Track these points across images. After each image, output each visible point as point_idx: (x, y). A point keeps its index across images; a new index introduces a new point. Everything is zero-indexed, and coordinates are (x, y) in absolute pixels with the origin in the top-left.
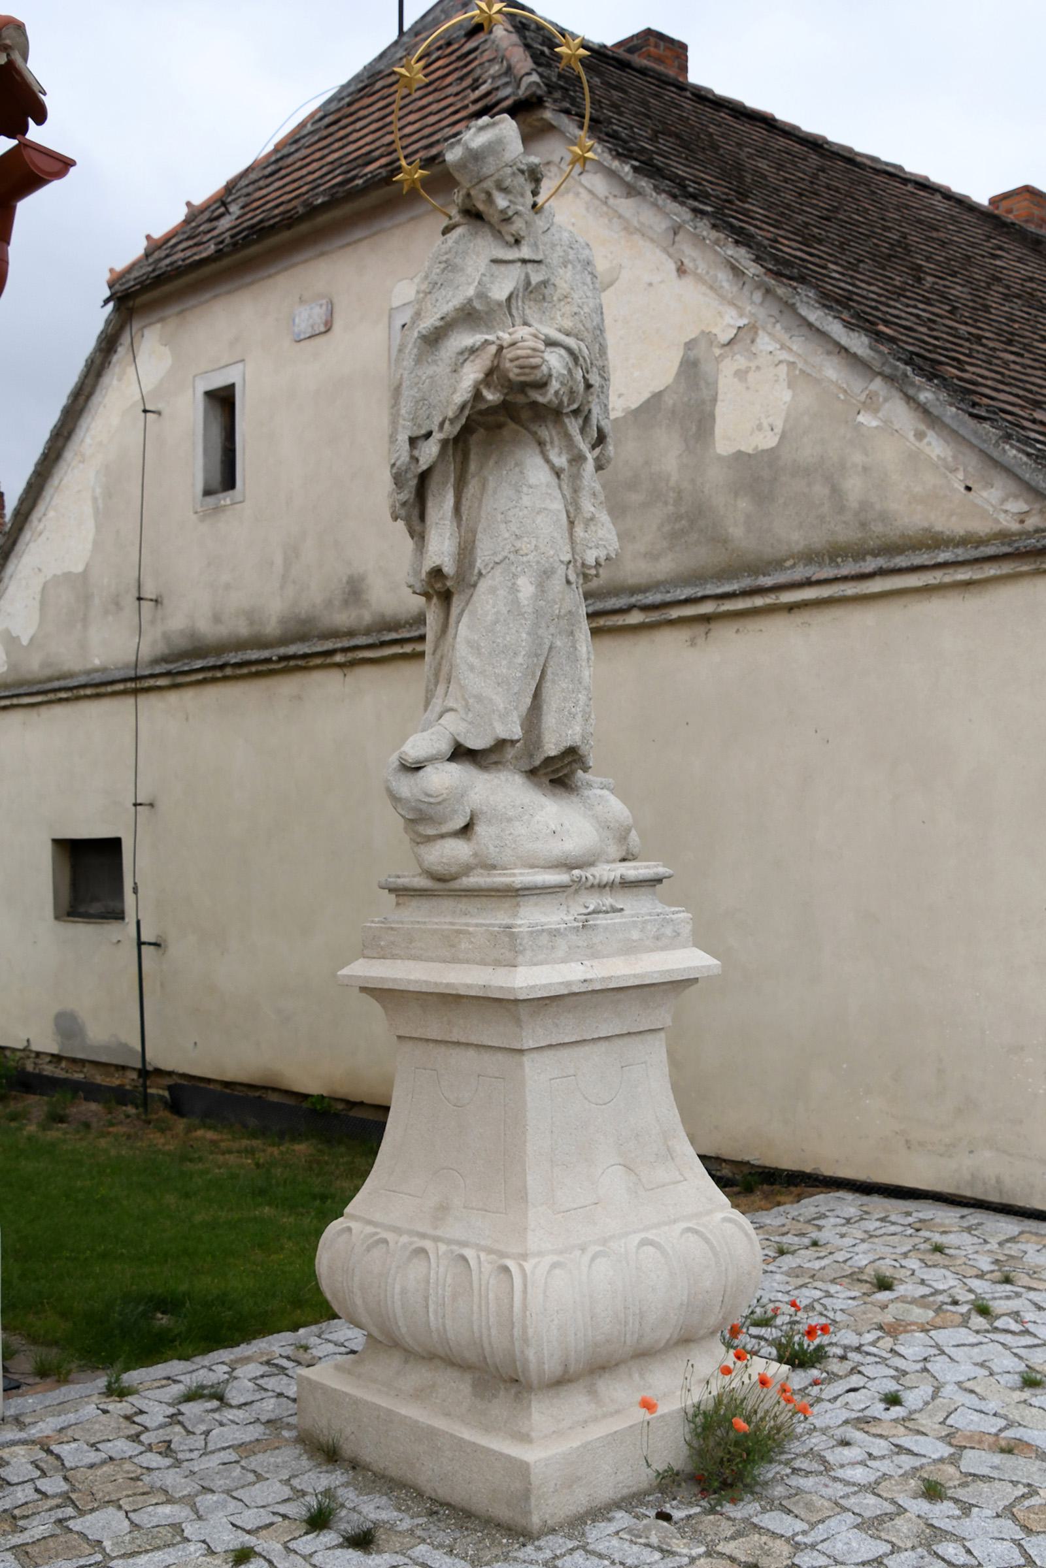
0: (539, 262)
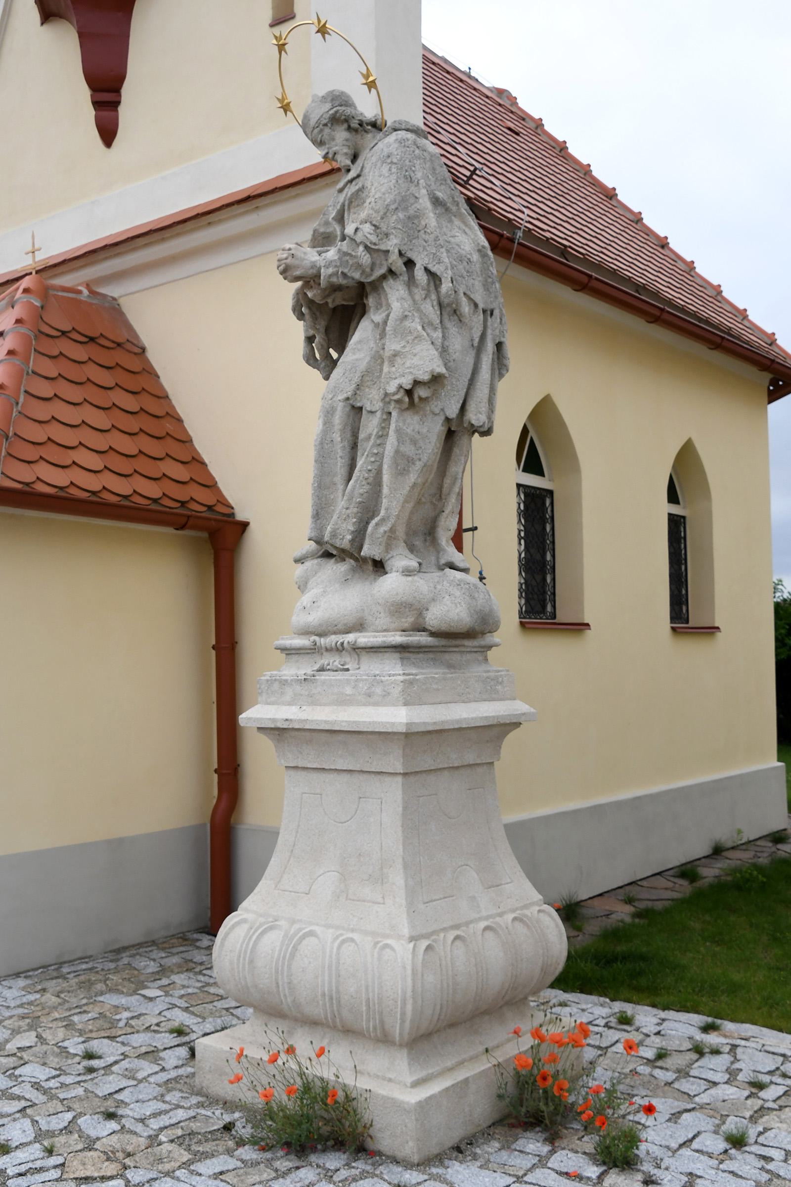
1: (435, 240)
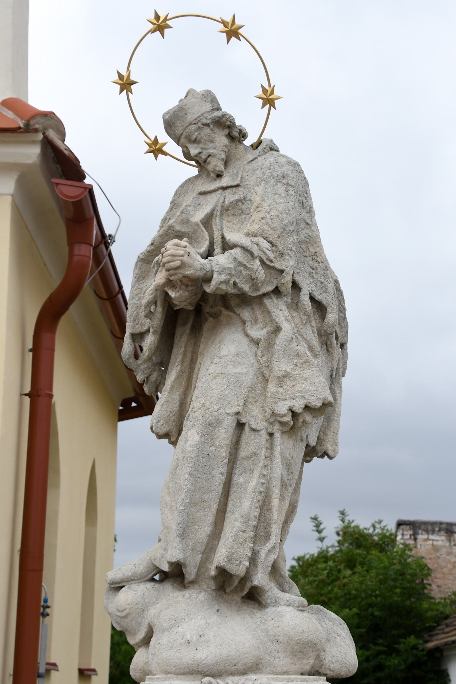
0: (238, 186)
1: (324, 269)
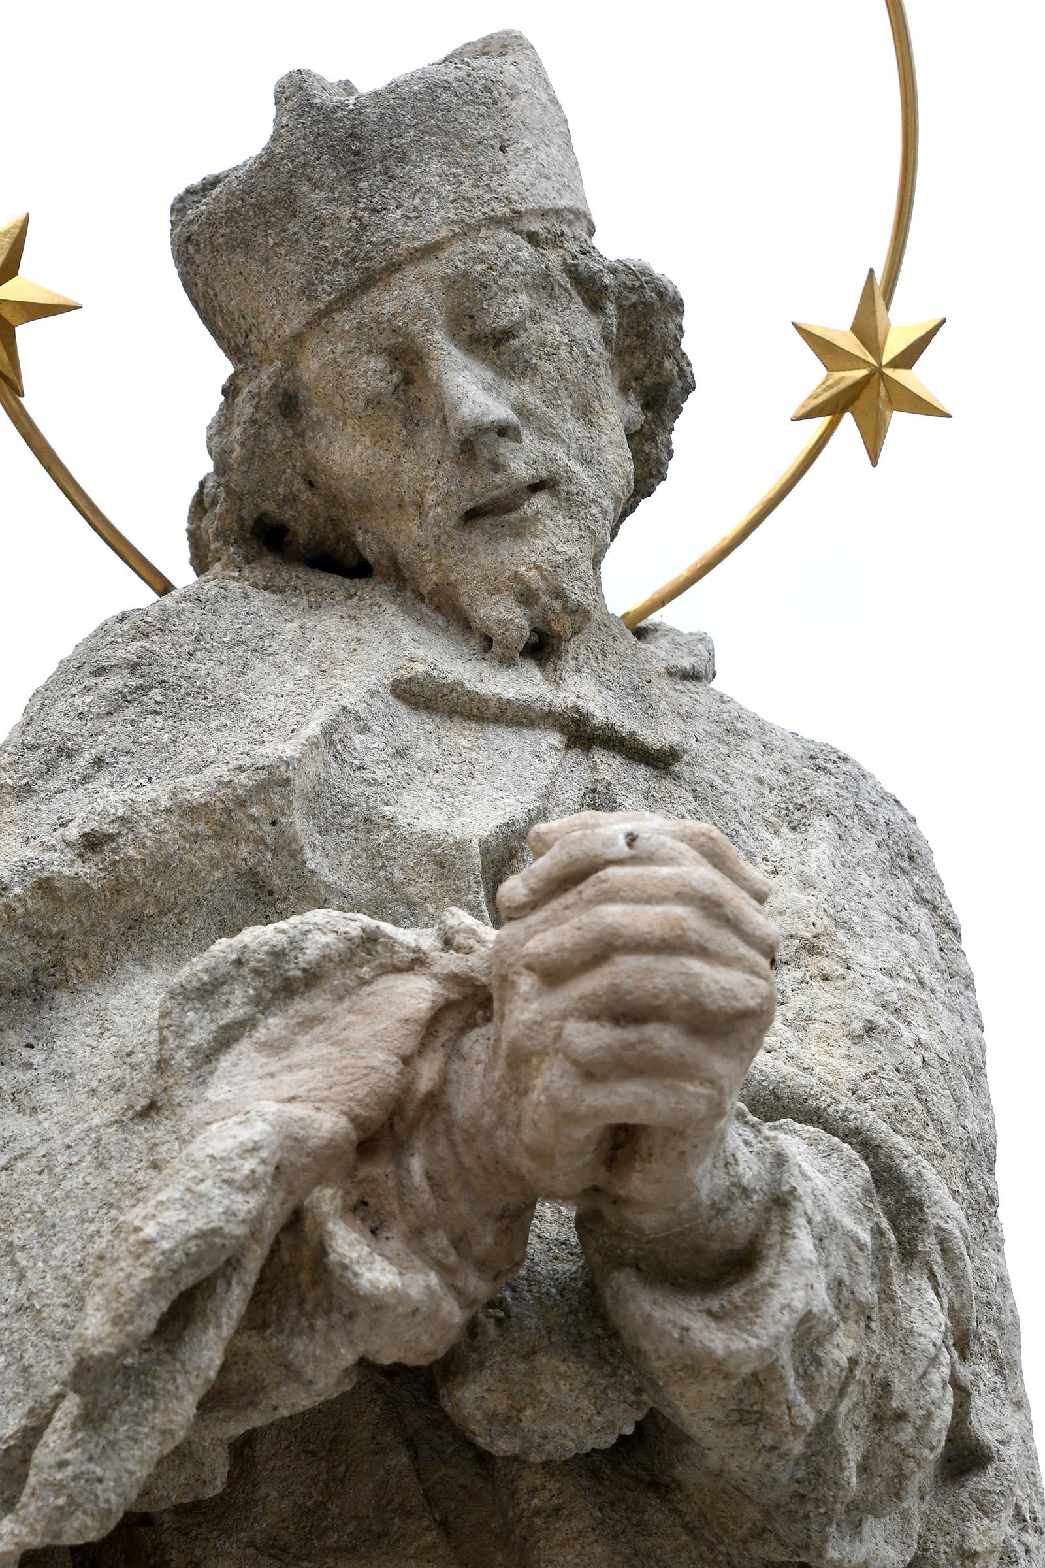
0: (662, 761)
